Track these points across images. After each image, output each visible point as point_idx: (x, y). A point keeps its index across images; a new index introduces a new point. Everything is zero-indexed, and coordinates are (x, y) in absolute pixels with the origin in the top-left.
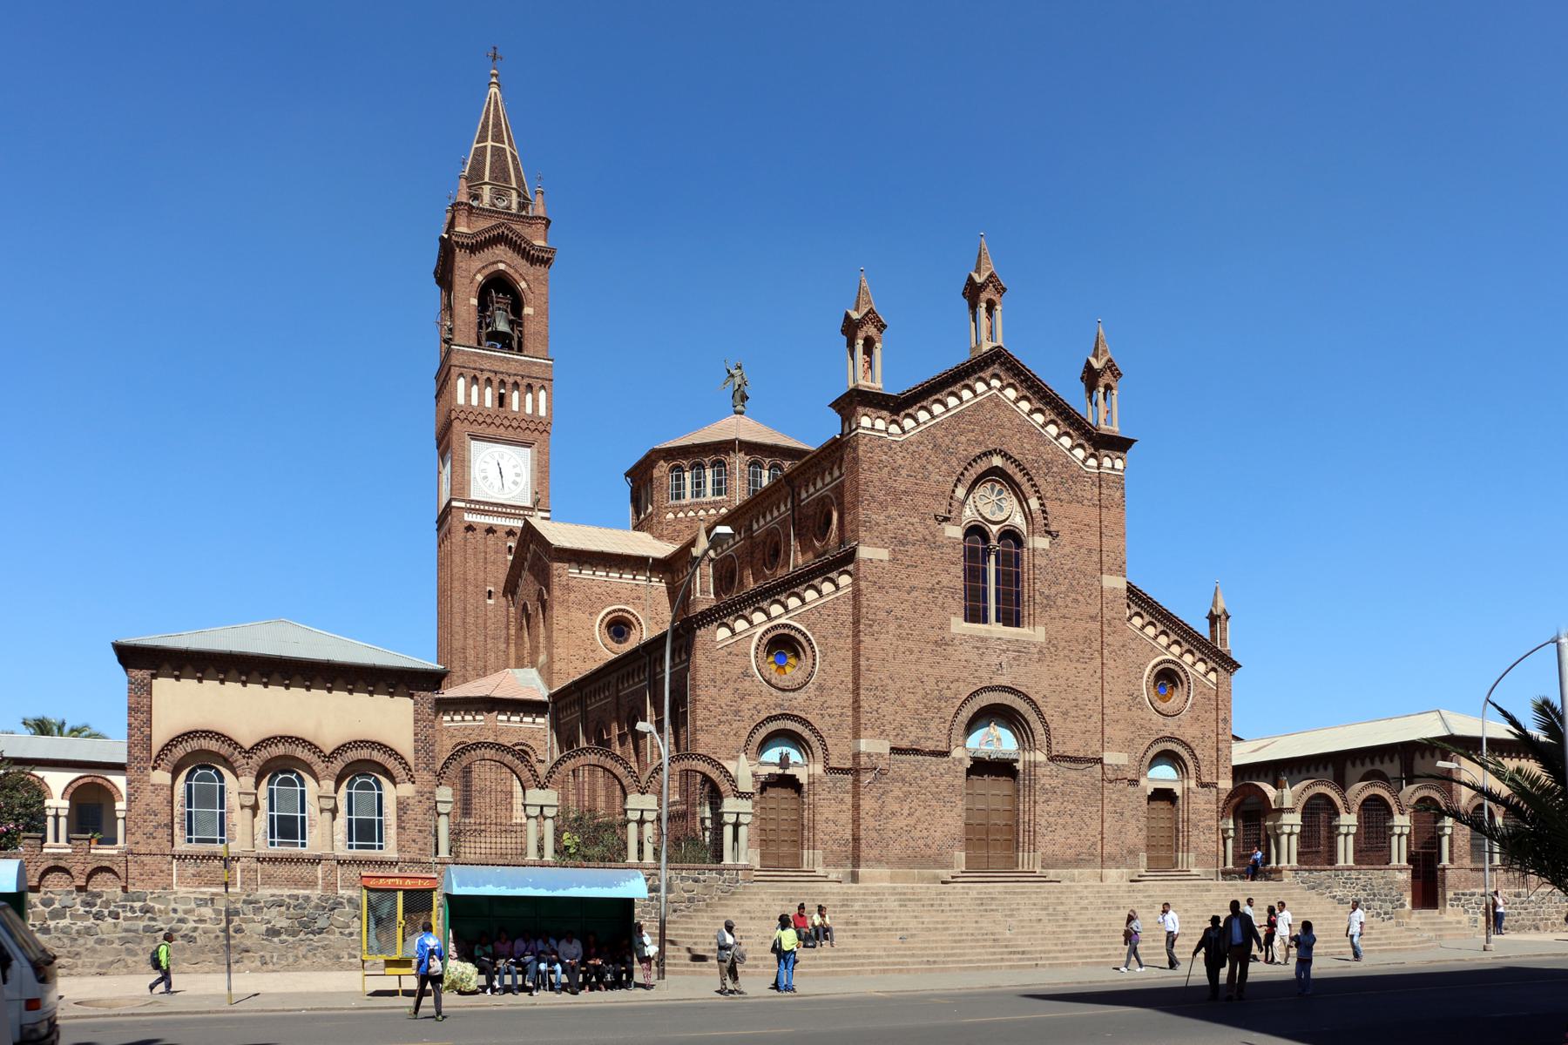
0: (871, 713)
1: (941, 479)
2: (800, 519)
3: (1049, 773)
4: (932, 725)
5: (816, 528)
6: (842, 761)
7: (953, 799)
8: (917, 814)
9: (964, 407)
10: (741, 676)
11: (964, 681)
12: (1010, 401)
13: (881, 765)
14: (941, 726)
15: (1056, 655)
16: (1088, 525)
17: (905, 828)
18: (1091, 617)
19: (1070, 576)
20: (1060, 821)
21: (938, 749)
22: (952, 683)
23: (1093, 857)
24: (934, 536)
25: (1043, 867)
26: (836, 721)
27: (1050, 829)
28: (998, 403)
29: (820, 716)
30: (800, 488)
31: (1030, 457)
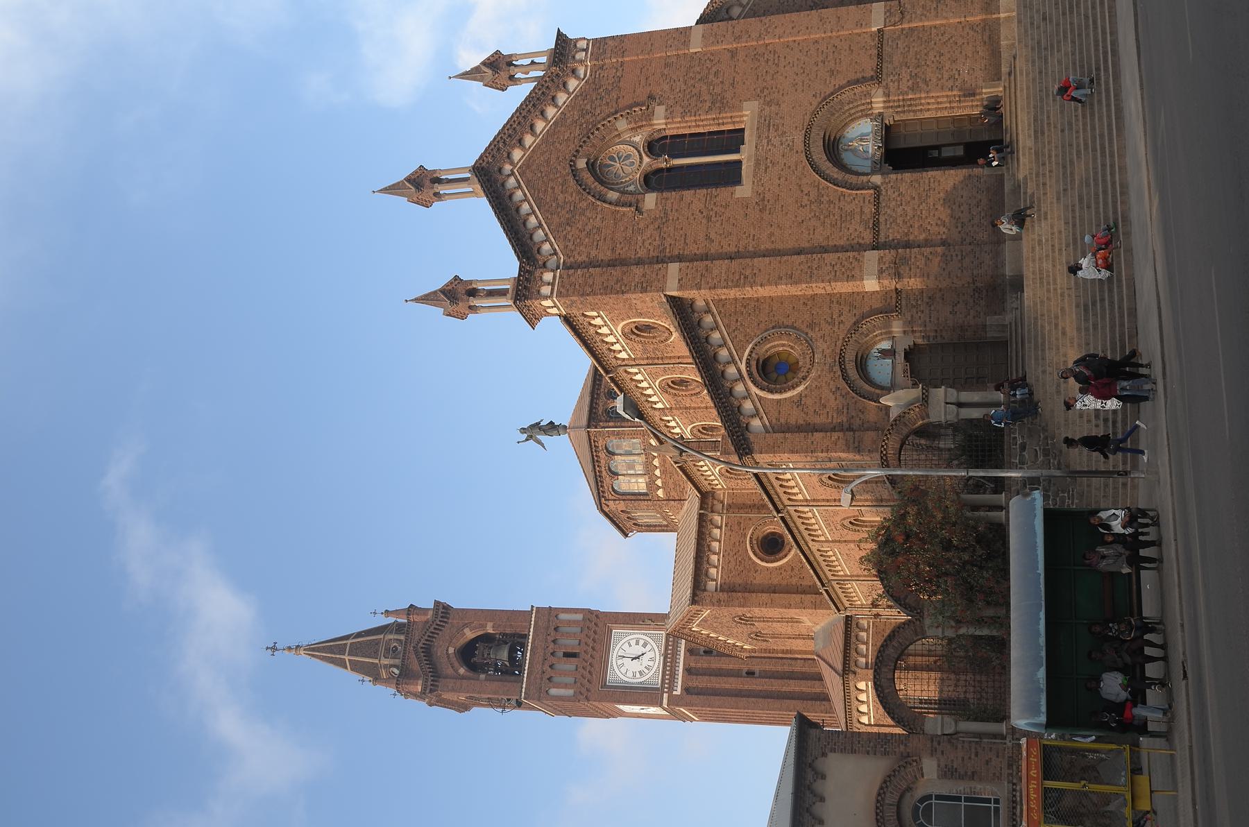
1: (599, 216)
2: (648, 358)
3: (896, 83)
4: (848, 208)
5: (654, 341)
7: (927, 182)
10: (800, 408)
11: (800, 179)
12: (524, 155)
15: (772, 88)
17: (960, 229)
19: (692, 82)
20: (948, 65)
22: (802, 191)
23: (987, 27)
24: (656, 219)
25: (999, 79)
26: (846, 309)
27: (957, 76)
28: (527, 165)
30: (616, 358)
31: (578, 132)
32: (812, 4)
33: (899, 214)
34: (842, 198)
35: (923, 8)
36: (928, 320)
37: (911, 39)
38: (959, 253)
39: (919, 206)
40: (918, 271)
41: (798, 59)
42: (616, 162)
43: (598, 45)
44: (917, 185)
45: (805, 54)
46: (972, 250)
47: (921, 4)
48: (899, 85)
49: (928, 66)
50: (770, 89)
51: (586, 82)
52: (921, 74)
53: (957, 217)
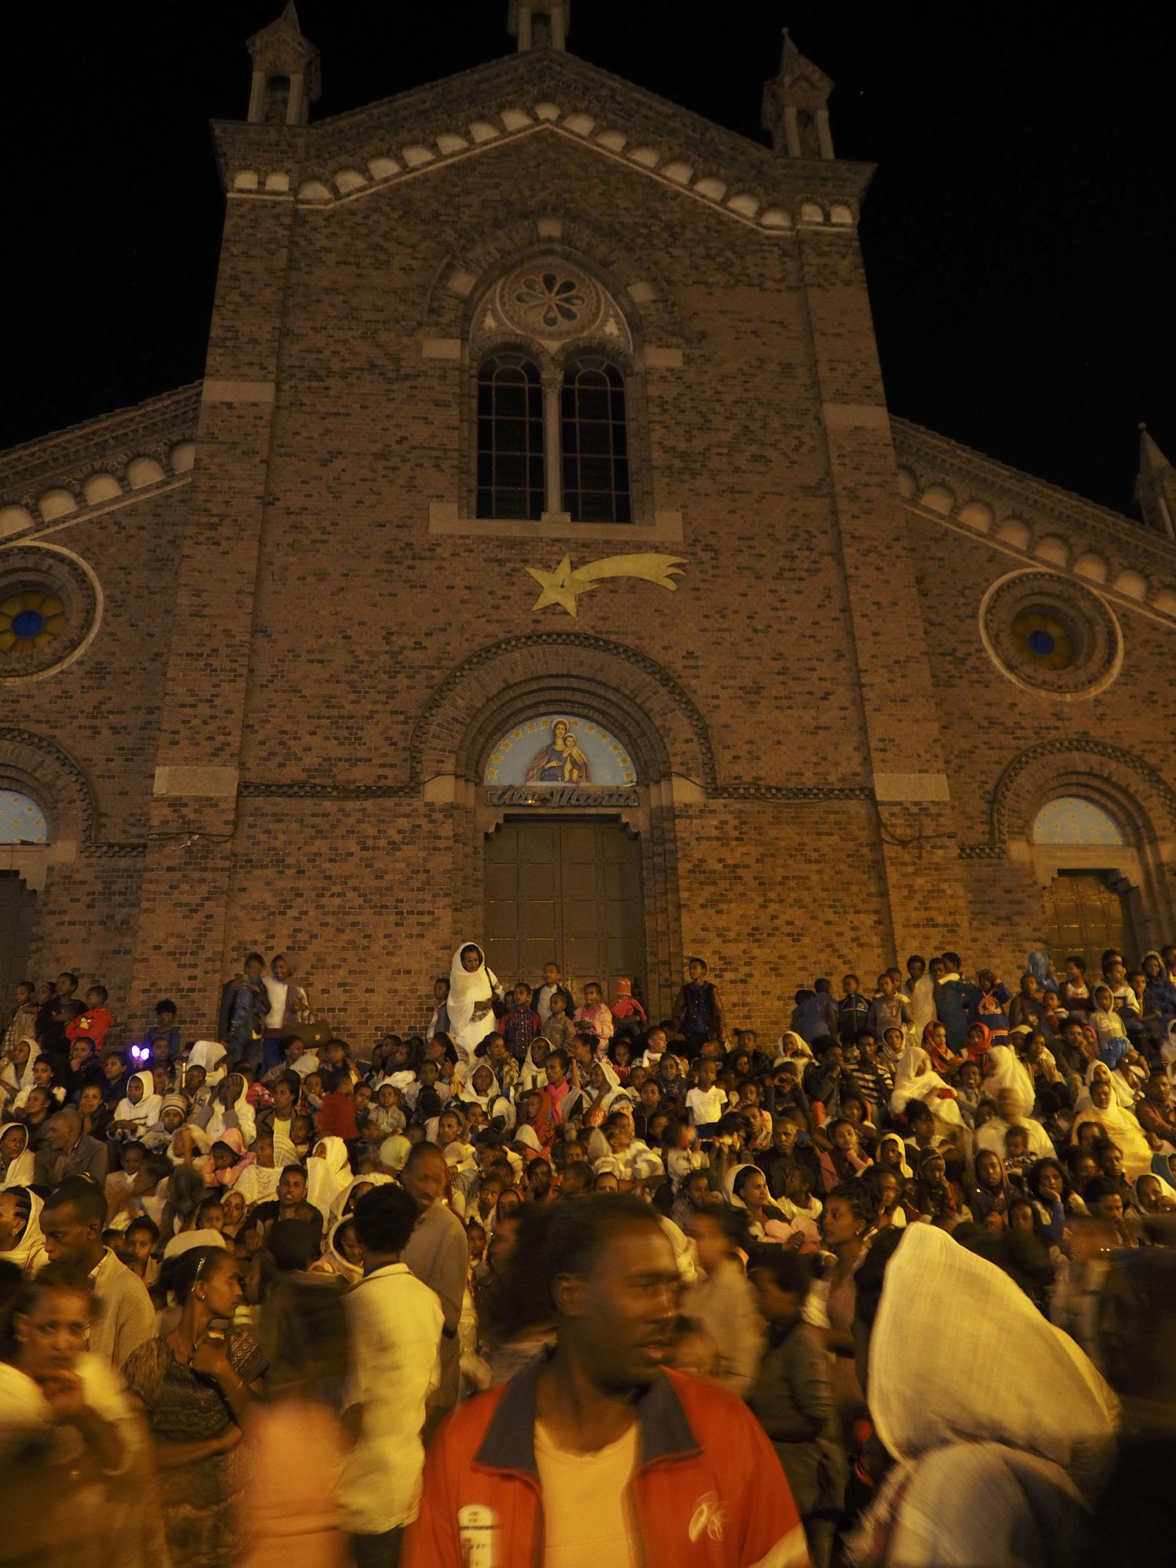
0: (194, 706)
1: (415, 264)
3: (715, 833)
6: (134, 831)
7: (427, 907)
8: (315, 947)
9: (477, 151)
13: (216, 823)
14: (394, 733)
15: (713, 567)
16: (781, 323)
18: (806, 489)
21: (383, 782)
22: (429, 634)
27: (730, 976)
29: (88, 732)
32: (959, 654)
33: (339, 843)
34: (401, 718)
35: (930, 892)
36: (67, 918)
37: (843, 867)
38: (197, 984)
39: (355, 889)
40: (166, 887)
41: (792, 619)
42: (558, 293)
43: (842, 242)
44: (415, 884)
45: (808, 633)
46: (204, 1015)
47: (944, 886)
48: (709, 839)
49: (763, 906)
50: (714, 563)
51: (752, 230)
52: (739, 888)
53: (312, 979)
